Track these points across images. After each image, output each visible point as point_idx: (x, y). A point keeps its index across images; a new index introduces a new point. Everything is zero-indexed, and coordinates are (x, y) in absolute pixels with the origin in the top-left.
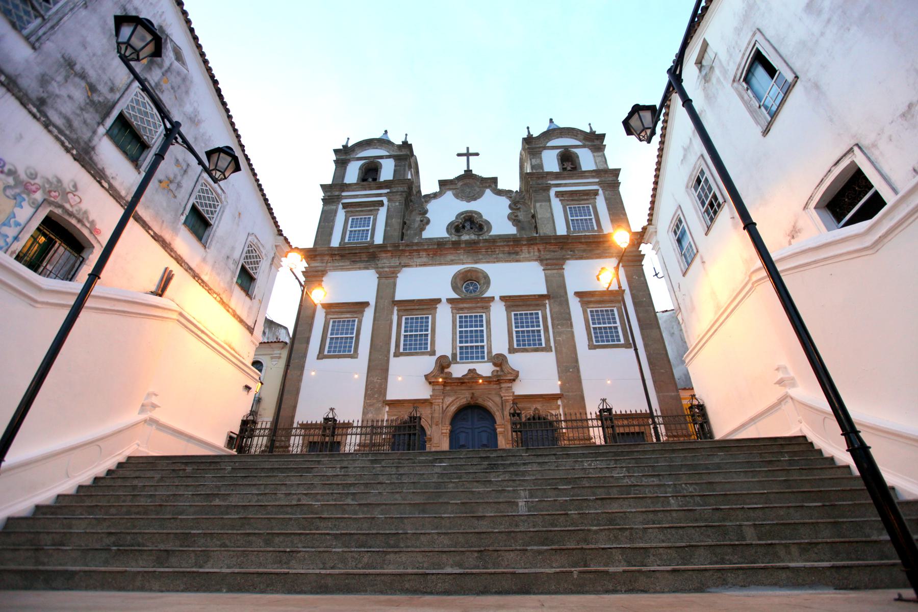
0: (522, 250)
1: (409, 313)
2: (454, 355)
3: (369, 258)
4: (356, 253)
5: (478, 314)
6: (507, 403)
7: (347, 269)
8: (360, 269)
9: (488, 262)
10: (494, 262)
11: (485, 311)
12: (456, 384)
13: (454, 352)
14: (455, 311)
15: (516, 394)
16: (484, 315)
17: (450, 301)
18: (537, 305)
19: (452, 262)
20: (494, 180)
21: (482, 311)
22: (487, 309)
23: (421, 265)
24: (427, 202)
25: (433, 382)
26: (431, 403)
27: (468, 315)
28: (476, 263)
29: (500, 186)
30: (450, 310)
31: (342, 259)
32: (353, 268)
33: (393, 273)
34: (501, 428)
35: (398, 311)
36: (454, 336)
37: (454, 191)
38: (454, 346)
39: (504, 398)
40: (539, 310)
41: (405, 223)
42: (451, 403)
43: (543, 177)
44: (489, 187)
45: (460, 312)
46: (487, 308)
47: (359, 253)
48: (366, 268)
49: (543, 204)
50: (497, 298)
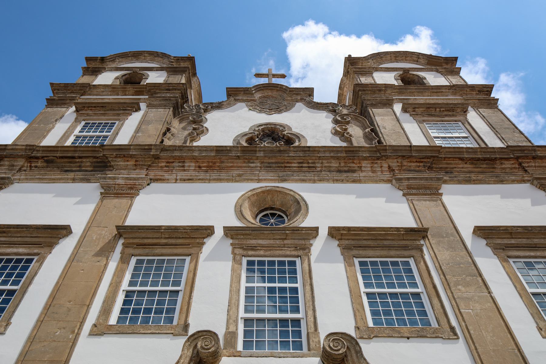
0: (361, 167)
1: (147, 251)
2: (231, 336)
3: (94, 167)
4: (73, 157)
5: (287, 259)
7: (50, 179)
8: (74, 180)
9: (303, 181)
10: (314, 181)
11: (300, 253)
13: (232, 329)
14: (238, 251)
16: (298, 261)
17: (229, 232)
18: (405, 248)
19: (239, 179)
20: (309, 92)
21: (295, 253)
22: (306, 249)
23: (184, 180)
24: (206, 111)
27: (266, 259)
28: (284, 180)
29: (317, 98)
30: (230, 248)
31: (47, 167)
32: (60, 179)
33: (131, 188)
35: (125, 246)
36: (235, 297)
37: (249, 104)
38: (233, 318)
40: (409, 257)
41: (168, 130)
43: (380, 90)
44: (302, 100)
45: (250, 253)
46: (304, 249)
47: (80, 157)
48: (88, 181)
49: (386, 118)
50: (323, 233)
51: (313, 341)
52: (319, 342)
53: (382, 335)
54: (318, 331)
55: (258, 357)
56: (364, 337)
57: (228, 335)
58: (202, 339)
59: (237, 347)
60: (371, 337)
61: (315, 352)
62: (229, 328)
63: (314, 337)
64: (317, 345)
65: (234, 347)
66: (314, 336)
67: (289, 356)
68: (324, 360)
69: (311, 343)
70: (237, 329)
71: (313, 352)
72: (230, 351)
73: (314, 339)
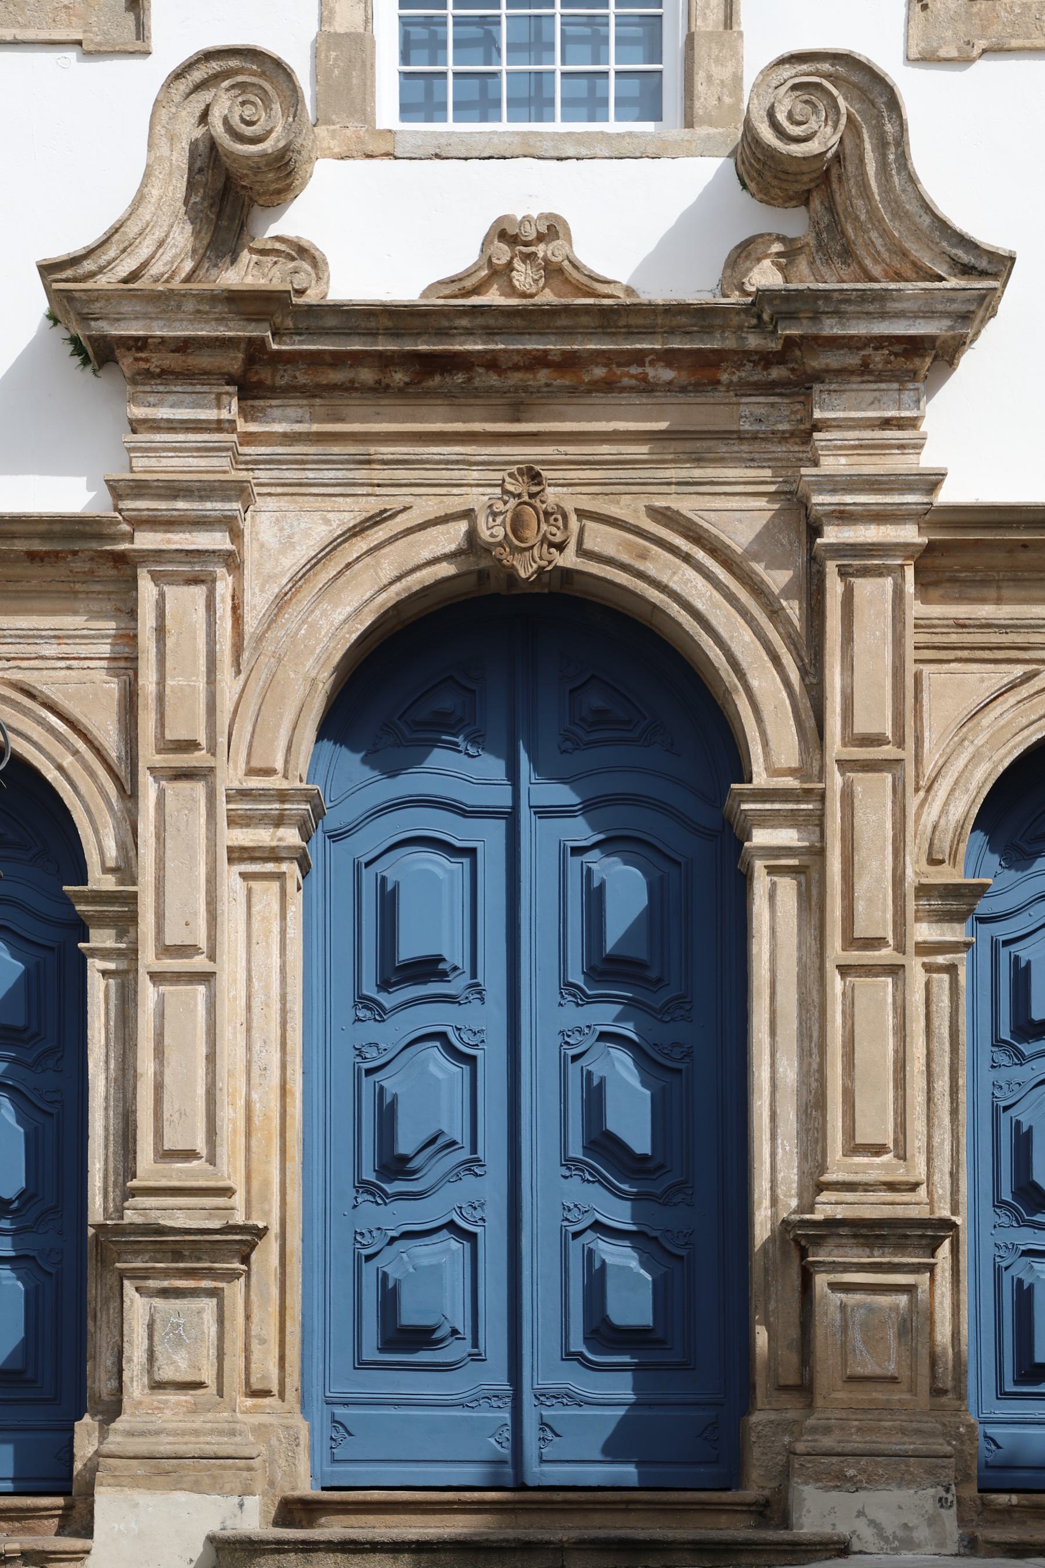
6: (863, 587)
12: (366, 375)
15: (947, 495)
25: (140, 344)
26: (120, 559)
34: (791, 819)
39: (832, 535)
42: (316, 562)
51: (709, 78)
52: (737, 80)
53: (1027, 43)
54: (735, 28)
55: (466, 159)
56: (943, 53)
57: (333, 54)
58: (227, 90)
59: (374, 120)
60: (976, 52)
61: (712, 131)
62: (332, 12)
63: (717, 60)
64: (727, 100)
65: (364, 112)
66: (715, 52)
67: (600, 153)
68: (748, 173)
69: (700, 87)
70: (368, 20)
71: (702, 131)
72: (348, 132)
73: (715, 70)
